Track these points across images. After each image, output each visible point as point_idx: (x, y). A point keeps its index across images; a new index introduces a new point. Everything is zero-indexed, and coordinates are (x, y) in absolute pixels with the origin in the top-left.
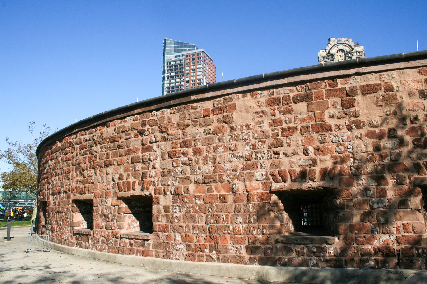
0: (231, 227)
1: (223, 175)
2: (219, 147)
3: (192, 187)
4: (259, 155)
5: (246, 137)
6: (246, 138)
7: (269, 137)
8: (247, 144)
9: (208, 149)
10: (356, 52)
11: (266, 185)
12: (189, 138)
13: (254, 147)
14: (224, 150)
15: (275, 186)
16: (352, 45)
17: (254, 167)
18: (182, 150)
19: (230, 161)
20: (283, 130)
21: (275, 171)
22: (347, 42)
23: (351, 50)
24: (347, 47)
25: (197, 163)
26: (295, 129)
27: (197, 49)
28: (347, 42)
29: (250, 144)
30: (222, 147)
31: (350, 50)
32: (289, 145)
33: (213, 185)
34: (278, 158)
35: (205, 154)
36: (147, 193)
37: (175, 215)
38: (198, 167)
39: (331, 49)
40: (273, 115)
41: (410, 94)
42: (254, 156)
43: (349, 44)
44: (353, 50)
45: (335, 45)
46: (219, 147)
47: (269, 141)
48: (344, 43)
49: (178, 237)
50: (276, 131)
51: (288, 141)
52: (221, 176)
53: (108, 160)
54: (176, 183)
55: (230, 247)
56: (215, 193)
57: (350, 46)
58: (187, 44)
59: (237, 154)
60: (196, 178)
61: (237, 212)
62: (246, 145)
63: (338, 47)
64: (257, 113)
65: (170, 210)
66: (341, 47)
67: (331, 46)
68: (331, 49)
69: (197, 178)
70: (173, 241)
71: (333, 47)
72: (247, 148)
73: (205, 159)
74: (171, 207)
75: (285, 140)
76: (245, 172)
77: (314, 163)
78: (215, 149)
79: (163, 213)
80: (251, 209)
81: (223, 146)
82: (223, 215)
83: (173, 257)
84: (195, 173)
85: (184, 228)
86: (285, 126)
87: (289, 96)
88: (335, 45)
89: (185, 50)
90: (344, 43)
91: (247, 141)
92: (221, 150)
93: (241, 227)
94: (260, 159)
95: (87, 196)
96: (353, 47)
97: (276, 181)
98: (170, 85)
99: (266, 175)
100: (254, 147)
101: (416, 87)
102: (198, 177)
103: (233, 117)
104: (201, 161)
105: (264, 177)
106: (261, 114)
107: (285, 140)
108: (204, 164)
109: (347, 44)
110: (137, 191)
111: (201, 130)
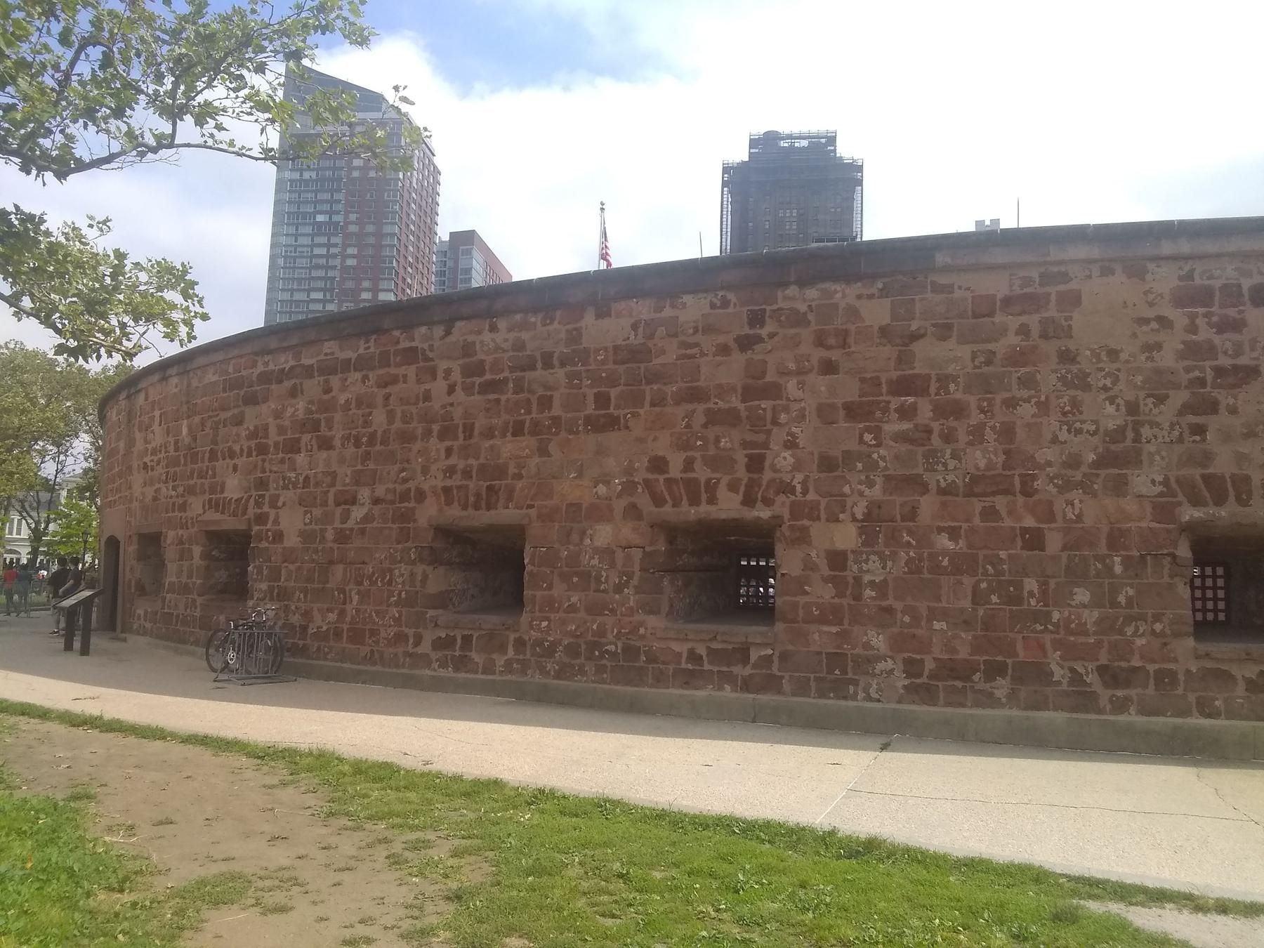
0: (1056, 616)
1: (1034, 478)
2: (1020, 403)
3: (928, 506)
4: (1146, 432)
5: (1108, 382)
6: (1109, 385)
7: (1177, 386)
8: (1112, 400)
9: (985, 404)
12: (919, 369)
14: (1036, 410)
15: (1189, 514)
17: (1132, 459)
18: (895, 402)
19: (1055, 440)
21: (1196, 473)
25: (948, 438)
29: (1119, 400)
30: (1032, 403)
32: (1233, 411)
33: (1000, 502)
34: (1204, 440)
35: (976, 418)
36: (763, 513)
37: (867, 578)
38: (948, 452)
40: (1192, 329)
42: (1130, 435)
46: (1020, 403)
47: (1179, 398)
49: (878, 641)
50: (1197, 373)
51: (1231, 401)
52: (1027, 481)
53: (604, 416)
54: (876, 492)
55: (1054, 667)
56: (1008, 522)
59: (1078, 425)
60: (942, 480)
62: (1107, 403)
64: (1144, 321)
65: (850, 563)
69: (945, 480)
70: (858, 651)
72: (1111, 409)
73: (977, 435)
74: (851, 557)
75: (1225, 398)
76: (1103, 473)
78: (1011, 404)
79: (826, 572)
80: (1118, 569)
81: (1034, 400)
82: (1031, 584)
83: (856, 693)
84: (940, 468)
85: (899, 615)
86: (1224, 361)
87: (1239, 286)
91: (1111, 393)
92: (1026, 411)
93: (1091, 617)
94: (1148, 442)
95: (505, 515)
97: (1196, 502)
99: (1166, 483)
100: (1133, 409)
102: (950, 478)
103: (1070, 327)
104: (963, 437)
105: (1160, 489)
106: (1154, 325)
107: (1225, 398)
108: (970, 443)
110: (728, 506)
111: (965, 351)
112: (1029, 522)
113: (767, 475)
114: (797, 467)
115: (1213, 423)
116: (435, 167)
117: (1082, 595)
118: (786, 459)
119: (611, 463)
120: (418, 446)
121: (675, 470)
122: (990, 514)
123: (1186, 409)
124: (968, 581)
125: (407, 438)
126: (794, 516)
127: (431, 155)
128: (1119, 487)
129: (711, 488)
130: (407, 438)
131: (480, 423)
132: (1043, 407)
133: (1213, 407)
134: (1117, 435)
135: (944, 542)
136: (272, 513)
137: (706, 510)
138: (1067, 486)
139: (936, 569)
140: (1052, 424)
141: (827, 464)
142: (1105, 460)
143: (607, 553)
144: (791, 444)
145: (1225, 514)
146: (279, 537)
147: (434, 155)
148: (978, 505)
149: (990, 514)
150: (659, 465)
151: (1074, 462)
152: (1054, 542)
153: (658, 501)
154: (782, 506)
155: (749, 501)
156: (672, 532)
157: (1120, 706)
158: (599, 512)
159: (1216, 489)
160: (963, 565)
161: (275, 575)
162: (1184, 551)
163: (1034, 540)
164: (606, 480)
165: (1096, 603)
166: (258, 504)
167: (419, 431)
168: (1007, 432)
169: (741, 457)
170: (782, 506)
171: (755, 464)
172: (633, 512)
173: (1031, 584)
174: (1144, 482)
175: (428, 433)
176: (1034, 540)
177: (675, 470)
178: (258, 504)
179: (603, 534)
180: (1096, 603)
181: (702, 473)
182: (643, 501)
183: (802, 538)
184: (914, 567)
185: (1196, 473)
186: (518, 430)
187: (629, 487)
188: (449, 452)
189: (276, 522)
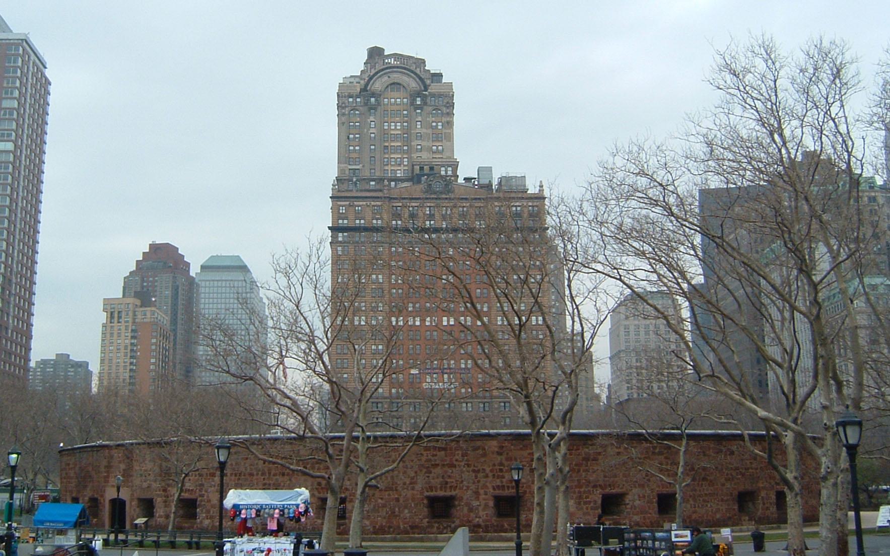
11: (422, 493)
15: (426, 494)
17: (415, 483)
20: (432, 465)
23: (423, 88)
24: (414, 78)
26: (437, 465)
33: (391, 492)
39: (371, 78)
43: (418, 72)
44: (426, 89)
45: (383, 70)
48: (405, 69)
56: (393, 496)
57: (420, 78)
61: (406, 507)
66: (396, 77)
68: (371, 78)
82: (397, 509)
88: (383, 70)
90: (405, 69)
93: (408, 515)
96: (428, 82)
109: (412, 72)
114: (350, 485)
116: (46, 79)
117: (406, 511)
118: (348, 483)
120: (255, 477)
122: (389, 495)
123: (426, 473)
124: (385, 509)
125: (251, 475)
126: (350, 496)
127: (41, 66)
128: (413, 489)
130: (251, 475)
131: (273, 472)
133: (431, 473)
134: (413, 478)
135: (380, 501)
136: (206, 494)
139: (379, 507)
142: (411, 483)
145: (432, 494)
146: (209, 501)
147: (45, 68)
148: (387, 493)
149: (389, 495)
151: (405, 484)
152: (401, 501)
153: (319, 493)
154: (347, 494)
159: (431, 489)
160: (384, 506)
161: (208, 512)
162: (425, 501)
163: (397, 500)
165: (409, 513)
166: (200, 491)
167: (255, 473)
170: (347, 494)
173: (397, 509)
174: (418, 487)
175: (257, 474)
176: (397, 500)
178: (200, 491)
180: (409, 513)
184: (374, 507)
185: (427, 486)
186: (283, 475)
188: (264, 479)
189: (208, 497)
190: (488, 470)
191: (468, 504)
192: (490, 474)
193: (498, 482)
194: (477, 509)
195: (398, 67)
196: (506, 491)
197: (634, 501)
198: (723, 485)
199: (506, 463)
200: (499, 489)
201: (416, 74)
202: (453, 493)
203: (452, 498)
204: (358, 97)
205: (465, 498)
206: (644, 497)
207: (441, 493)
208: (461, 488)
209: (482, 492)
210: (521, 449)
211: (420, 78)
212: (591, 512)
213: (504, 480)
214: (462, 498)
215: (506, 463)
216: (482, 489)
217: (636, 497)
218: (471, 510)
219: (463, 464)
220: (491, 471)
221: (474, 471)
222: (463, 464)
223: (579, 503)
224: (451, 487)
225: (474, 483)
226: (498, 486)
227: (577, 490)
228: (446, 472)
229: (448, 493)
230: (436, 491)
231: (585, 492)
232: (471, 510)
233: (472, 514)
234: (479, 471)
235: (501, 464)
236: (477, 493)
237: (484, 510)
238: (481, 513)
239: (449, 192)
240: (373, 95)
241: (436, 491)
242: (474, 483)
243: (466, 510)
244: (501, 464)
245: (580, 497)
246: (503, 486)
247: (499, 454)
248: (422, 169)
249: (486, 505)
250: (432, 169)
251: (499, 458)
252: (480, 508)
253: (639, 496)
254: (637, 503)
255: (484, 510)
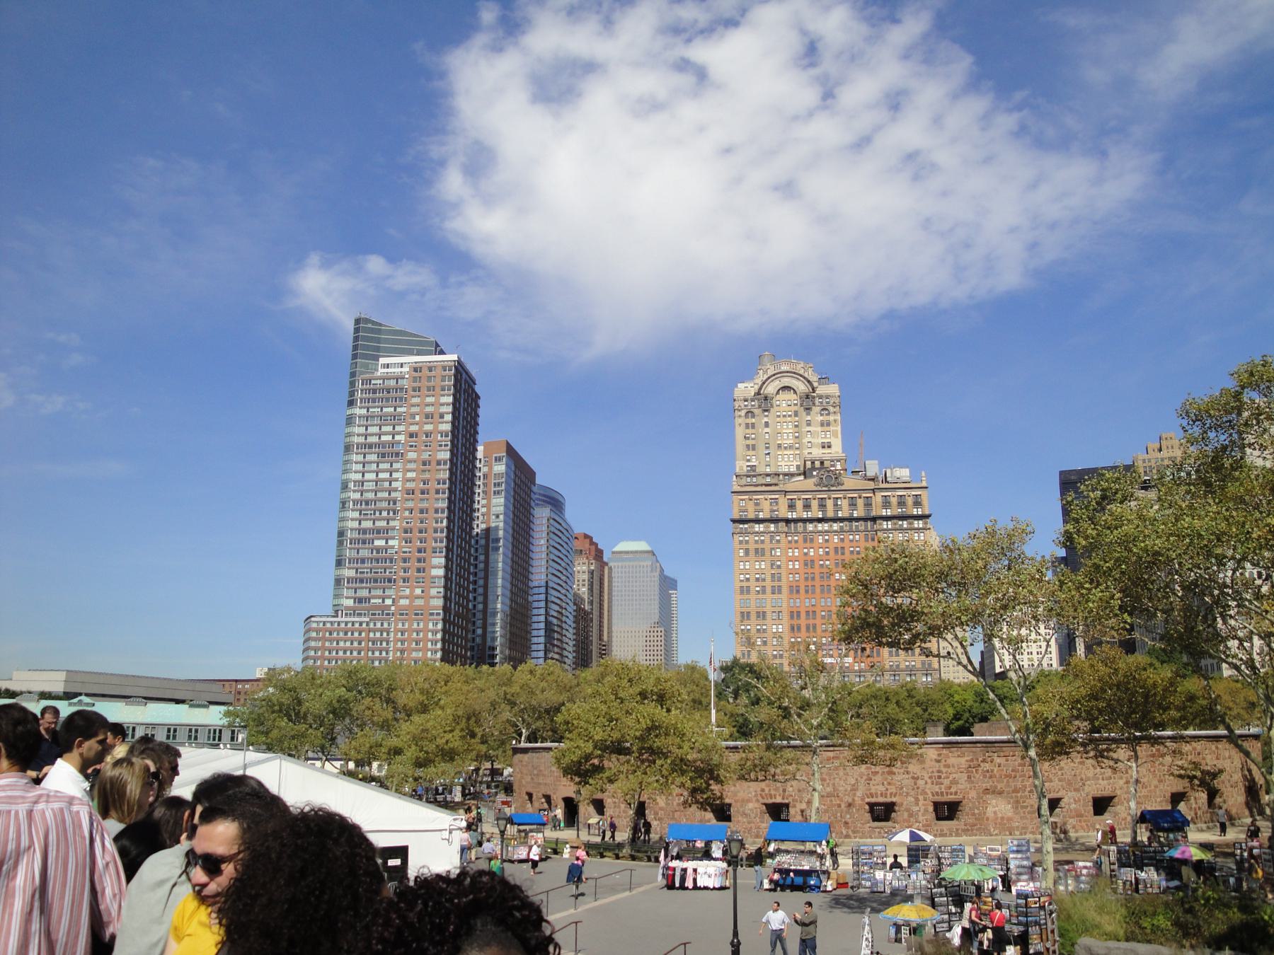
10: (821, 397)
11: (863, 799)
13: (857, 780)
15: (867, 800)
16: (814, 378)
17: (857, 789)
21: (868, 792)
22: (803, 370)
26: (878, 772)
27: (442, 352)
28: (801, 372)
31: (807, 391)
33: (833, 798)
36: (787, 801)
39: (764, 383)
41: (931, 760)
43: (806, 375)
44: (814, 391)
45: (774, 375)
47: (865, 777)
48: (794, 373)
57: (809, 381)
58: (418, 336)
63: (783, 380)
66: (786, 381)
67: (766, 377)
68: (764, 383)
71: (769, 378)
77: (887, 790)
78: (834, 779)
88: (774, 375)
89: (410, 353)
90: (794, 373)
92: (837, 780)
96: (815, 384)
98: (366, 439)
100: (857, 780)
101: (935, 757)
107: (873, 778)
109: (801, 376)
110: (779, 800)
112: (838, 802)
113: (787, 793)
114: (793, 791)
115: (871, 782)
116: (477, 394)
118: (791, 789)
119: (751, 789)
121: (767, 791)
122: (831, 801)
127: (472, 383)
129: (775, 795)
132: (840, 779)
133: (871, 780)
134: (853, 785)
137: (773, 801)
138: (845, 795)
140: (842, 782)
141: (799, 791)
143: (751, 810)
144: (792, 786)
150: (763, 790)
151: (846, 791)
152: (843, 806)
153: (763, 798)
155: (783, 799)
156: (766, 805)
157: (855, 837)
158: (749, 801)
162: (867, 807)
163: (839, 806)
164: (751, 793)
168: (834, 784)
169: (781, 789)
171: (784, 791)
172: (758, 801)
173: (839, 814)
174: (859, 794)
177: (767, 791)
179: (751, 805)
181: (773, 792)
182: (760, 798)
183: (795, 806)
185: (868, 792)
187: (756, 796)
190: (926, 778)
191: (908, 810)
192: (929, 781)
193: (937, 789)
194: (917, 814)
195: (788, 372)
196: (945, 797)
197: (1069, 804)
198: (1156, 787)
199: (944, 770)
200: (938, 795)
201: (804, 378)
202: (894, 800)
203: (893, 804)
204: (752, 400)
205: (905, 803)
206: (1079, 800)
207: (881, 800)
208: (900, 794)
209: (921, 798)
210: (959, 756)
211: (809, 381)
212: (1028, 816)
213: (943, 786)
214: (902, 804)
215: (944, 770)
216: (921, 794)
217: (1072, 800)
218: (911, 815)
219: (902, 771)
220: (930, 777)
221: (913, 778)
222: (902, 771)
223: (1017, 808)
224: (891, 794)
225: (913, 789)
226: (937, 793)
227: (1013, 795)
228: (886, 779)
229: (889, 800)
230: (877, 797)
231: (1021, 797)
232: (911, 815)
233: (912, 819)
234: (918, 778)
235: (939, 771)
236: (917, 800)
237: (923, 815)
238: (921, 818)
239: (839, 484)
240: (766, 398)
241: (877, 797)
242: (913, 789)
243: (906, 815)
244: (939, 771)
245: (1017, 802)
246: (942, 793)
247: (939, 761)
248: (813, 463)
249: (926, 810)
250: (822, 463)
251: (937, 765)
252: (920, 814)
253: (1075, 800)
254: (1073, 806)
255: (923, 815)
